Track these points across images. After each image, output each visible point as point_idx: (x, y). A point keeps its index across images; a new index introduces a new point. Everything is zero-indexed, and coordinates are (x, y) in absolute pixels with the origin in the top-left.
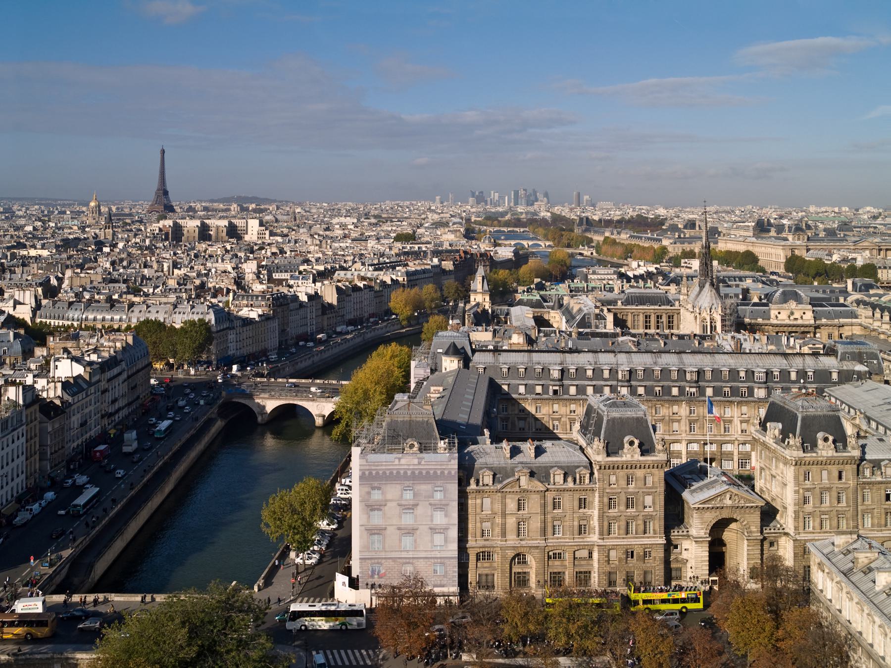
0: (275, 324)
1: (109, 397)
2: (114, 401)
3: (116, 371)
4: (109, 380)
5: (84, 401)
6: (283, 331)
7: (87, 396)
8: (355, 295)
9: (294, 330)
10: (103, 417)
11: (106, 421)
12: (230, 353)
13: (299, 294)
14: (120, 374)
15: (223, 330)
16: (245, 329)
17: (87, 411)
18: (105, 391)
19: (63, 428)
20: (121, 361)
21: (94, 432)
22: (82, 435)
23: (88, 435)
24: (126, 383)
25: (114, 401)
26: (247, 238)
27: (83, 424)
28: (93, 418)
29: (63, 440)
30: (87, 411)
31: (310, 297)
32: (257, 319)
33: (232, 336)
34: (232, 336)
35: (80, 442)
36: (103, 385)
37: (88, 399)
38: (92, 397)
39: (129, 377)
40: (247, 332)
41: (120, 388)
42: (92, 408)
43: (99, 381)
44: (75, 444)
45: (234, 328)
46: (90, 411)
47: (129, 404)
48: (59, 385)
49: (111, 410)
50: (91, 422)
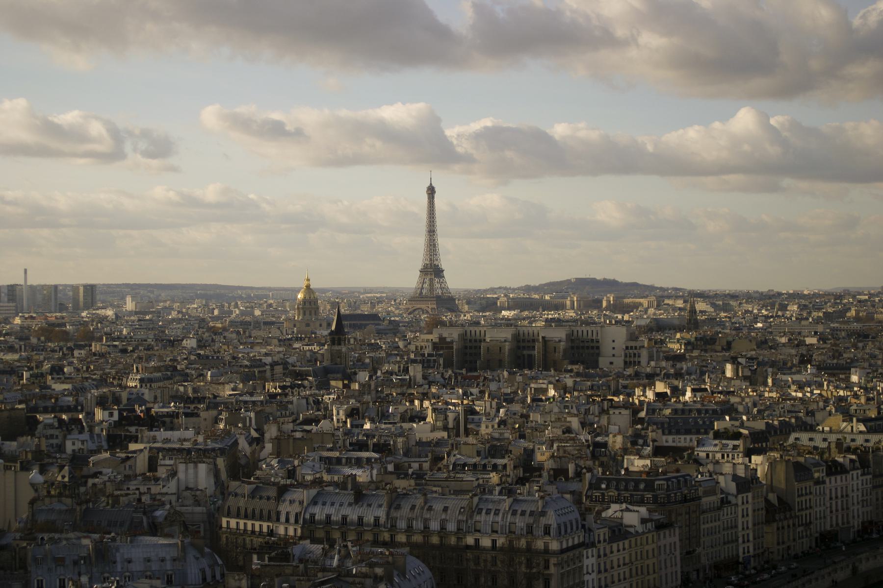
0: (672, 538)
6: (688, 554)
8: (835, 483)
15: (574, 547)
16: (615, 546)
26: (603, 362)
32: (640, 529)
34: (590, 561)
40: (619, 553)
45: (593, 545)
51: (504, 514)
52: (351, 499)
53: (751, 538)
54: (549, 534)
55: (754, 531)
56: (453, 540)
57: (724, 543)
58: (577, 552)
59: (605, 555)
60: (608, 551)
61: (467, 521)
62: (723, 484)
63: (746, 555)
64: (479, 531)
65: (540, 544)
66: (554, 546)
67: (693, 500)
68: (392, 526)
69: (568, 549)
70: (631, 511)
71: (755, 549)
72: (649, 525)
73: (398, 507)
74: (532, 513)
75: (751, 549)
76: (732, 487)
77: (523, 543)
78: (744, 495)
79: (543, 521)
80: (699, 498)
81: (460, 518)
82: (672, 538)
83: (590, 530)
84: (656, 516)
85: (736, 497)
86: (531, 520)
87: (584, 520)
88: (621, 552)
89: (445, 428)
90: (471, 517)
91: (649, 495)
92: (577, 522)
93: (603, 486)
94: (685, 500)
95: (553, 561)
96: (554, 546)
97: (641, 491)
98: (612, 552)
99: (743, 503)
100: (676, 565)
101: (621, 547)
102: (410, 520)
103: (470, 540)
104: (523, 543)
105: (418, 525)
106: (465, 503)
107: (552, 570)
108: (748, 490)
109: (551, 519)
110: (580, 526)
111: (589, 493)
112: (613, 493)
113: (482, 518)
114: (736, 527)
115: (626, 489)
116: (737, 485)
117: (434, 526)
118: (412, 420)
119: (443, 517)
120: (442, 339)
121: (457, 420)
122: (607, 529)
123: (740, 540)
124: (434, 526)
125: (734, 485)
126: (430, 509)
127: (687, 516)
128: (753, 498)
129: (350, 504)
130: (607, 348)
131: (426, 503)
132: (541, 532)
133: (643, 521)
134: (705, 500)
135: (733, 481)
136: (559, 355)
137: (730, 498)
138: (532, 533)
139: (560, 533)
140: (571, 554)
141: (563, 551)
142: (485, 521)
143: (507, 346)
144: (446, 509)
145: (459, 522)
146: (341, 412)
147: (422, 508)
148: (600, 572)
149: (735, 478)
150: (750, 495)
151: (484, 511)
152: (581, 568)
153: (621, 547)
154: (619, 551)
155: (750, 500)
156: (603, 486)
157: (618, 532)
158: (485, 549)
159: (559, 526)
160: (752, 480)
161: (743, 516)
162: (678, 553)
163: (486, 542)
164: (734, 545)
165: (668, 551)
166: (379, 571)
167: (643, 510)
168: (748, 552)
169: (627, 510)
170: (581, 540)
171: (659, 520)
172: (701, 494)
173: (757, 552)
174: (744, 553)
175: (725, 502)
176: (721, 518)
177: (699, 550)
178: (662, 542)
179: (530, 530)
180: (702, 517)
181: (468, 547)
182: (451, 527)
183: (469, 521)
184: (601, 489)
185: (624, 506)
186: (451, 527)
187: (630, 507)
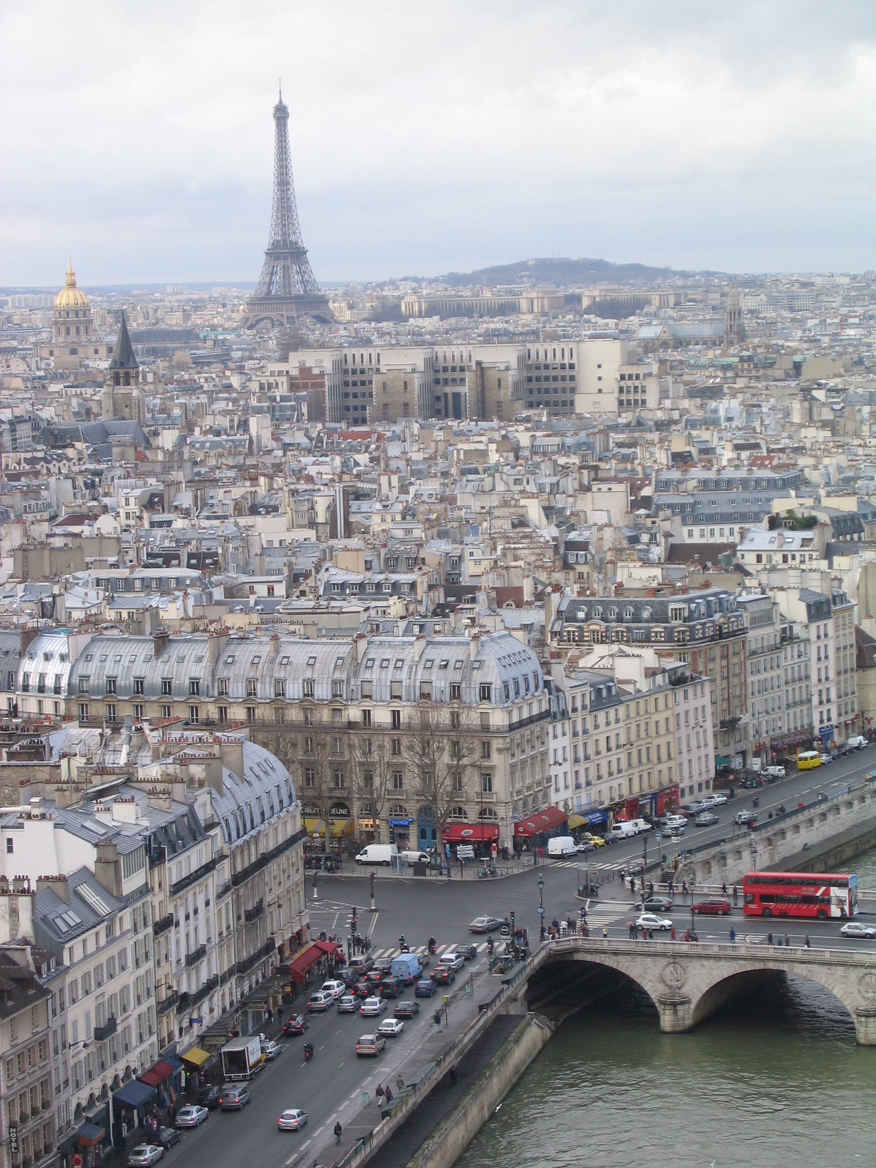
0: (700, 702)
1: (179, 942)
2: (195, 958)
3: (195, 857)
4: (178, 887)
5: (103, 958)
6: (728, 726)
7: (112, 939)
9: (763, 720)
10: (163, 1008)
11: (173, 1022)
12: (558, 798)
13: (780, 597)
14: (208, 868)
15: (531, 720)
16: (601, 716)
17: (112, 987)
18: (164, 925)
19: (43, 1043)
20: (211, 826)
21: (139, 1055)
22: (103, 1067)
23: (120, 1068)
24: (229, 898)
25: (195, 958)
26: (583, 404)
27: (104, 1032)
28: (135, 1011)
29: (45, 1083)
30: (112, 987)
31: (819, 610)
32: (644, 685)
33: (559, 742)
35: (96, 1087)
36: (159, 903)
37: (114, 950)
38: (128, 943)
39: (237, 879)
40: (610, 725)
41: (206, 918)
42: (128, 978)
43: (145, 890)
44: (83, 1096)
45: (564, 714)
46: (125, 989)
47: (242, 968)
48: (24, 903)
49: (188, 985)
50: (130, 1022)
51: (411, 668)
52: (149, 649)
53: (833, 696)
54: (489, 698)
55: (838, 683)
56: (325, 715)
57: (788, 706)
58: (536, 727)
59: (585, 732)
60: (590, 725)
62: (783, 608)
63: (826, 724)
64: (370, 697)
65: (471, 719)
66: (498, 719)
67: (734, 634)
69: (521, 724)
70: (627, 656)
71: (840, 715)
72: (659, 679)
75: (834, 715)
77: (443, 717)
78: (821, 623)
79: (478, 677)
80: (744, 631)
81: (337, 675)
82: (700, 702)
83: (558, 690)
84: (671, 663)
85: (807, 627)
86: (457, 677)
87: (549, 673)
88: (613, 725)
89: (312, 524)
90: (356, 674)
91: (659, 628)
92: (536, 676)
93: (581, 615)
94: (720, 634)
95: (496, 744)
96: (498, 719)
97: (647, 621)
98: (596, 727)
99: (819, 637)
100: (706, 745)
101: (612, 718)
102: (251, 682)
103: (354, 714)
104: (443, 717)
105: (266, 690)
106: (344, 651)
107: (497, 759)
108: (827, 615)
109: (493, 675)
110: (541, 684)
111: (557, 628)
112: (598, 626)
113: (373, 675)
114: (807, 677)
115: (620, 620)
116: (809, 607)
117: (294, 690)
118: (254, 510)
119: (308, 675)
120: (37, 478)
121: (332, 510)
122: (588, 689)
123: (815, 700)
124: (294, 690)
125: (803, 605)
126: (286, 663)
127: (724, 663)
128: (837, 628)
129: (148, 660)
130: (587, 379)
133: (651, 673)
134: (751, 634)
136: (506, 393)
137: (797, 630)
138: (459, 697)
139: (507, 697)
140: (526, 731)
141: (512, 728)
142: (380, 680)
143: (416, 382)
144: (312, 663)
145: (335, 682)
146: (132, 501)
147: (272, 661)
148: (576, 760)
149: (804, 592)
150: (830, 623)
151: (377, 663)
152: (544, 754)
153: (612, 718)
154: (608, 724)
155: (831, 631)
156: (581, 615)
157: (606, 694)
158: (380, 729)
160: (834, 597)
161: (819, 659)
162: (709, 725)
163: (382, 716)
164: (805, 708)
165: (692, 722)
166: (197, 771)
167: (649, 656)
168: (829, 719)
170: (545, 707)
171: (674, 670)
172: (747, 624)
173: (842, 719)
174: (822, 722)
175: (787, 638)
176: (783, 663)
177: (745, 718)
178: (681, 709)
179: (456, 691)
180: (748, 663)
181: (351, 725)
182: (323, 691)
183: (352, 682)
184: (574, 619)
185: (615, 648)
186: (323, 691)
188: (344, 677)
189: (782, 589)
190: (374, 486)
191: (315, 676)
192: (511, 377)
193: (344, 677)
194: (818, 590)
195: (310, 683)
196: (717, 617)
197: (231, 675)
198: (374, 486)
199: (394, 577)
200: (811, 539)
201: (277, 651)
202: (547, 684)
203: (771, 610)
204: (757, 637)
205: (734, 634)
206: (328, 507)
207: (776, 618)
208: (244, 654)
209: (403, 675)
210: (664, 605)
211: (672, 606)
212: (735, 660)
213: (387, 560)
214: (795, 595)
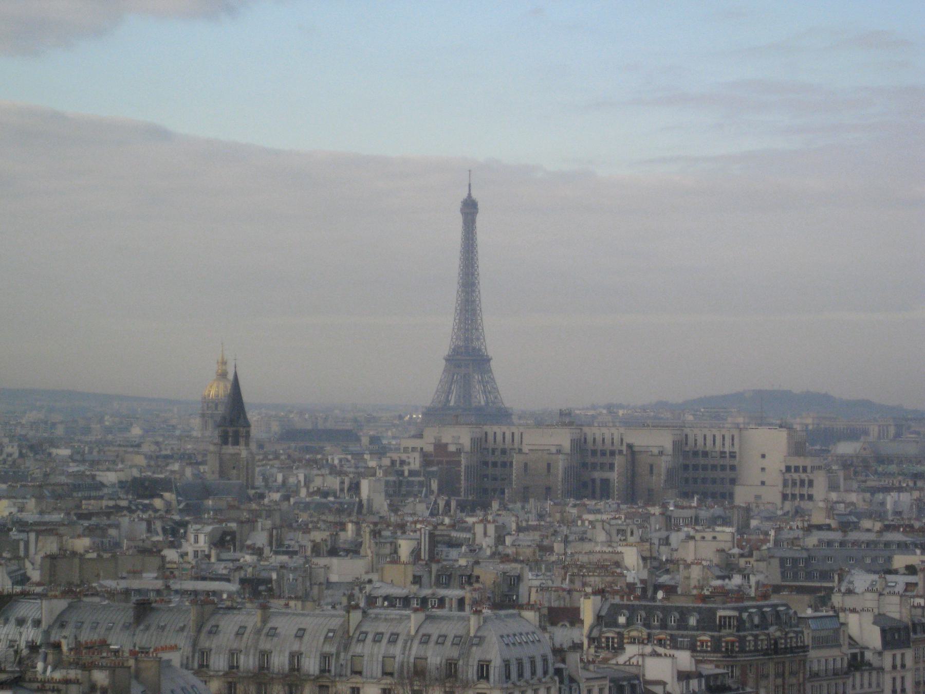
26: (742, 496)
51: (406, 642)
54: (487, 678)
61: (338, 655)
64: (360, 673)
68: (201, 666)
70: (659, 655)
72: (694, 684)
73: (214, 631)
74: (459, 641)
76: (872, 637)
78: (898, 653)
79: (477, 654)
80: (805, 648)
83: (572, 680)
84: (709, 669)
85: (880, 654)
86: (454, 653)
87: (563, 661)
90: (346, 647)
92: (545, 660)
93: (622, 620)
94: (775, 649)
97: (693, 629)
99: (894, 667)
102: (233, 653)
106: (335, 623)
108: (904, 643)
110: (551, 671)
111: (595, 633)
112: (638, 631)
115: (664, 626)
116: (883, 631)
119: (295, 648)
122: (607, 683)
125: (877, 631)
126: (273, 633)
127: (779, 681)
128: (916, 660)
129: (126, 627)
130: (750, 471)
131: (265, 621)
132: (472, 673)
134: (812, 654)
135: (875, 623)
136: (658, 480)
137: (868, 656)
138: (456, 676)
139: (508, 677)
142: (372, 655)
143: (561, 464)
144: (300, 634)
145: (325, 657)
146: (202, 538)
149: (880, 619)
150: (909, 654)
151: (370, 637)
155: (909, 662)
156: (622, 620)
159: (507, 664)
160: (914, 624)
167: (685, 659)
169: (655, 654)
171: (716, 676)
172: (808, 640)
175: (857, 663)
180: (808, 686)
182: (311, 665)
183: (342, 655)
184: (615, 624)
185: (648, 649)
186: (311, 665)
187: (660, 650)
188: (333, 650)
189: (853, 611)
190: (468, 535)
191: (303, 649)
192: (664, 463)
193: (333, 650)
194: (896, 616)
195: (295, 657)
196: (772, 629)
197: (213, 646)
198: (468, 535)
199: (442, 592)
200: (916, 584)
201: (265, 621)
202: (558, 672)
203: (836, 631)
204: (818, 658)
205: (792, 650)
206: (413, 552)
207: (844, 641)
208: (229, 624)
209: (397, 650)
210: (713, 611)
211: (720, 613)
212: (794, 680)
213: (438, 577)
214: (868, 618)
